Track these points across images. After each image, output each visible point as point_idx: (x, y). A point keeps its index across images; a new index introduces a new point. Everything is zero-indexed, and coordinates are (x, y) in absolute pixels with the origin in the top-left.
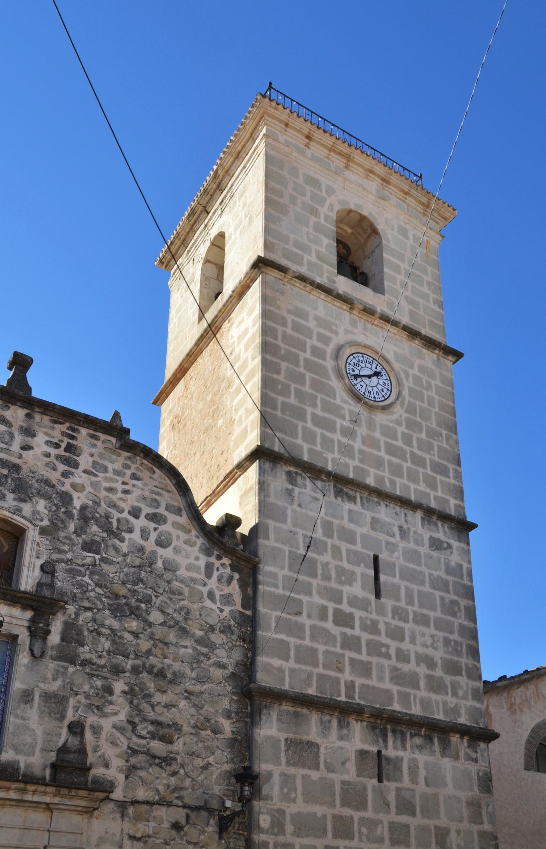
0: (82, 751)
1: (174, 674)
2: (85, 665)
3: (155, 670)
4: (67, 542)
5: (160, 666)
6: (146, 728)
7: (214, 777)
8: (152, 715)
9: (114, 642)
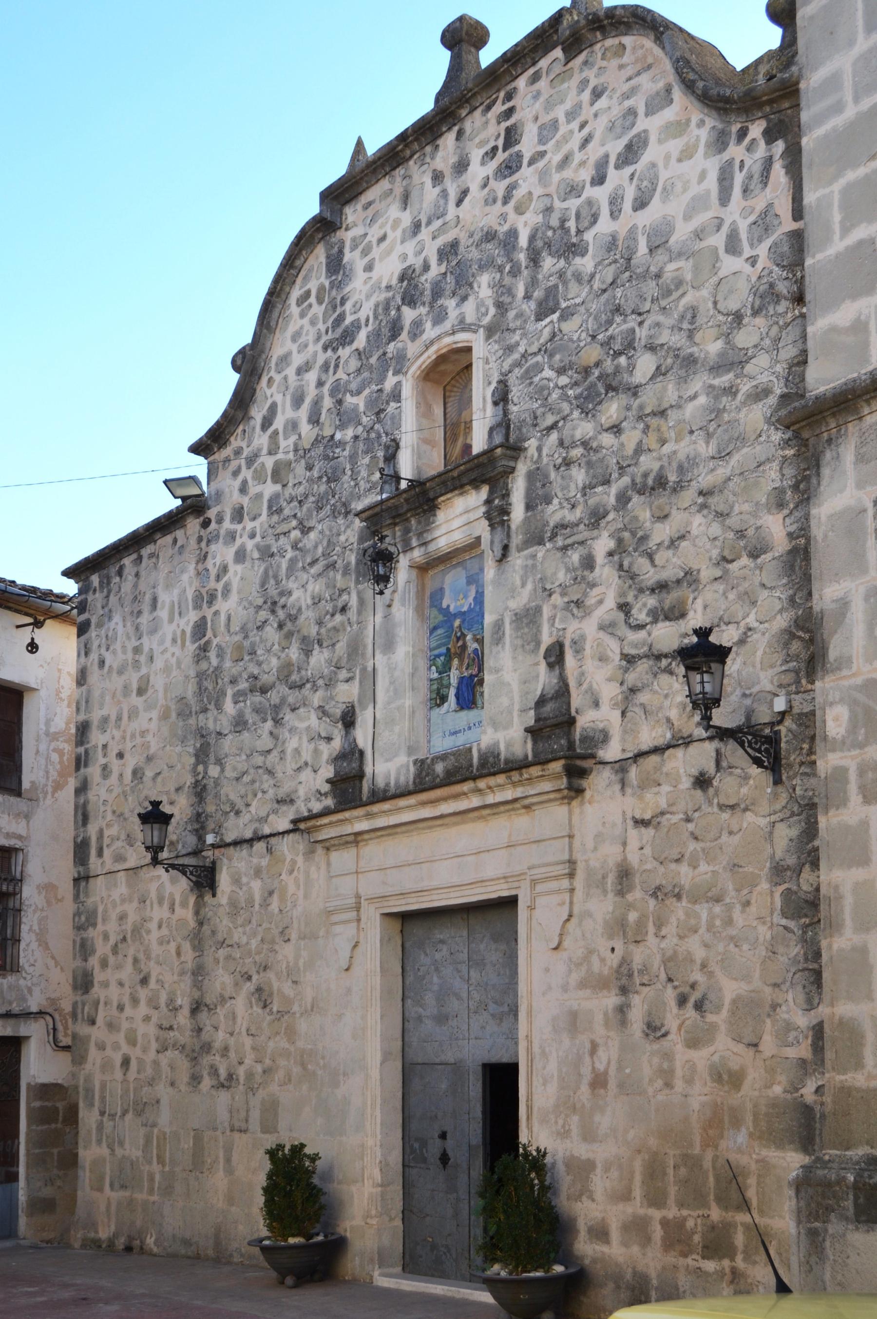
0: (563, 692)
1: (681, 469)
3: (650, 482)
4: (518, 323)
5: (656, 466)
6: (645, 605)
7: (759, 653)
8: (650, 575)
9: (590, 464)
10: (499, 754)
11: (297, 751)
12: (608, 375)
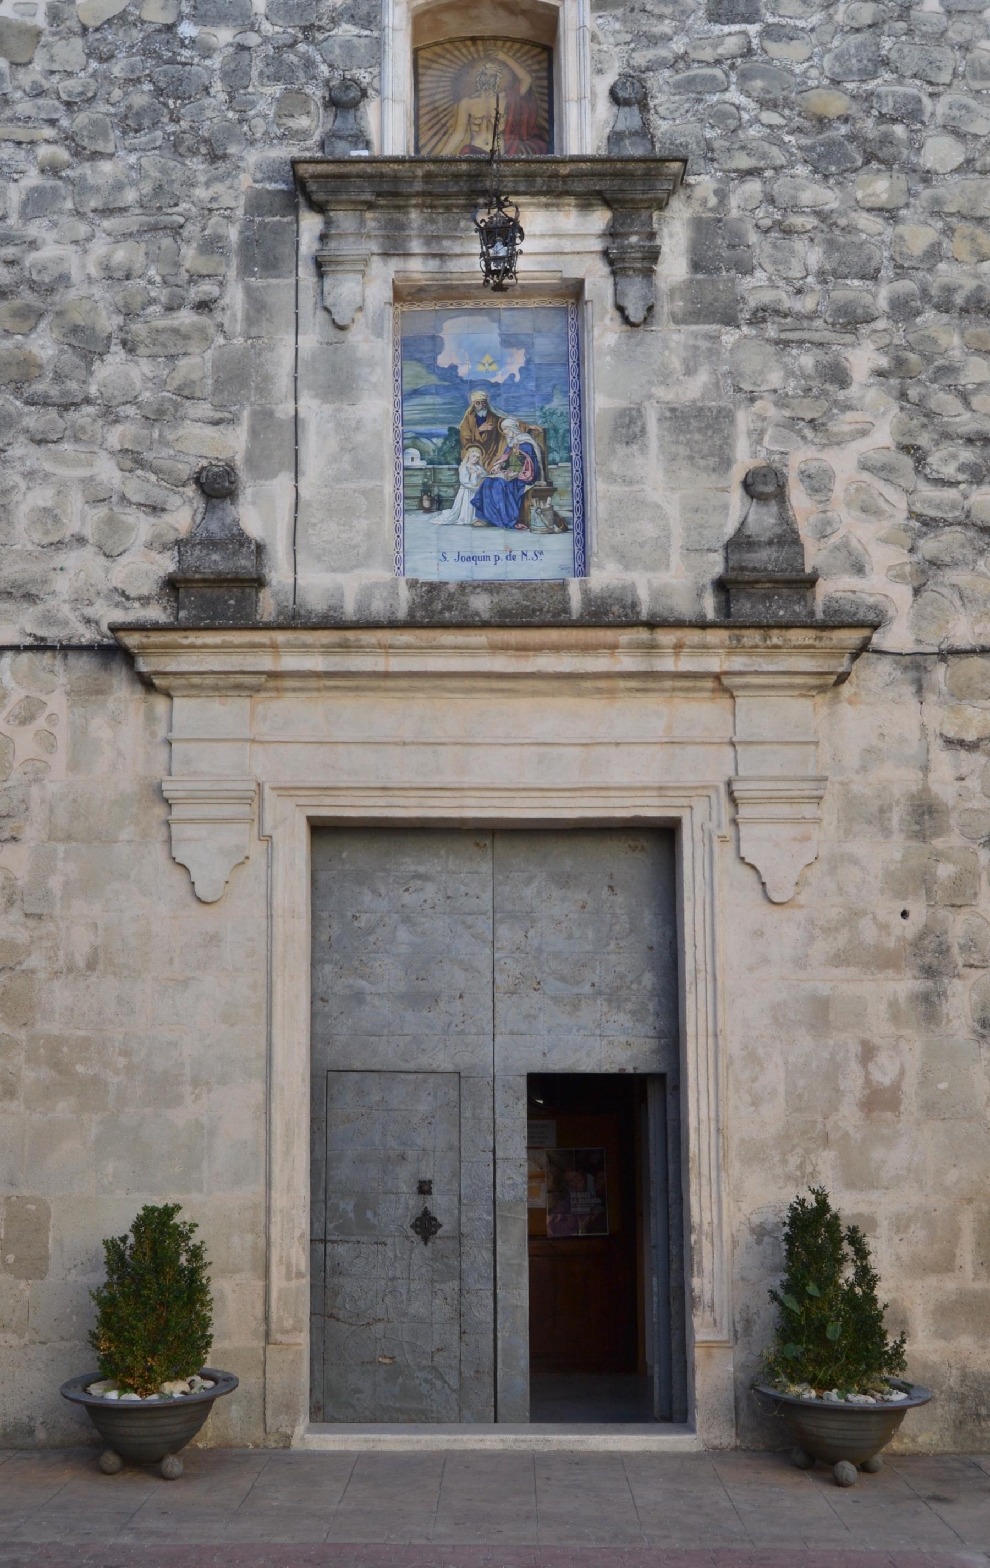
2: (764, 320)
9: (831, 245)
10: (634, 605)
11: (50, 515)
12: (866, 140)
